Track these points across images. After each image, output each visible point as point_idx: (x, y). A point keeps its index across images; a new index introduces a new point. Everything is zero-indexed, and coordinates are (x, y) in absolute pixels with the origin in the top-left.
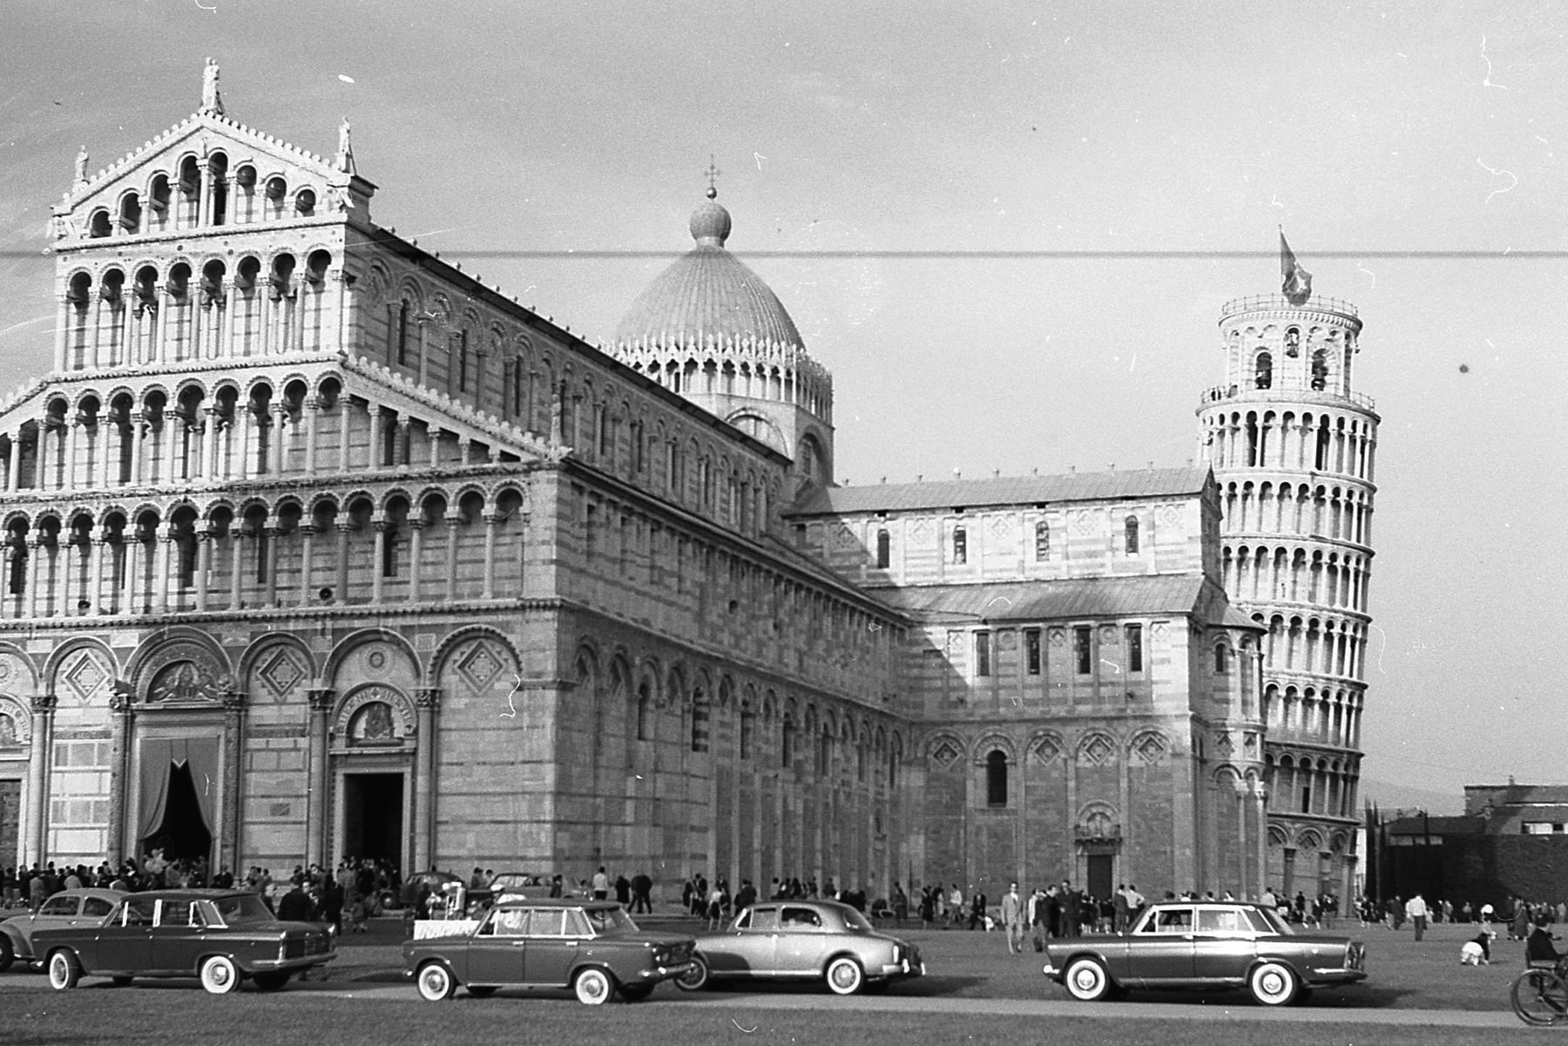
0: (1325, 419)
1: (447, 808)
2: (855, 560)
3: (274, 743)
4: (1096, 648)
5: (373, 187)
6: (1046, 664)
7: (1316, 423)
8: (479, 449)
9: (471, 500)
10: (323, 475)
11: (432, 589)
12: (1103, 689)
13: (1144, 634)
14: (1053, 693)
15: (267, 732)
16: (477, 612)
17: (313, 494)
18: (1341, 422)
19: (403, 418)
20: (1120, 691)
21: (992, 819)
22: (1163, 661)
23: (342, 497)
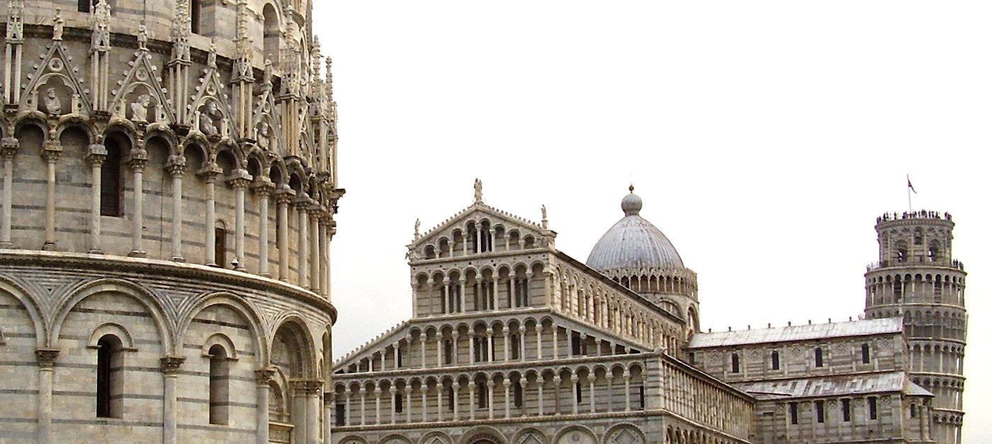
0: (938, 277)
2: (721, 369)
4: (853, 410)
5: (556, 233)
6: (827, 417)
7: (934, 279)
8: (620, 349)
9: (617, 370)
10: (545, 361)
11: (599, 407)
12: (857, 428)
13: (877, 402)
14: (831, 431)
16: (625, 417)
17: (543, 369)
18: (947, 278)
19: (583, 336)
20: (867, 429)
22: (887, 414)
23: (556, 370)
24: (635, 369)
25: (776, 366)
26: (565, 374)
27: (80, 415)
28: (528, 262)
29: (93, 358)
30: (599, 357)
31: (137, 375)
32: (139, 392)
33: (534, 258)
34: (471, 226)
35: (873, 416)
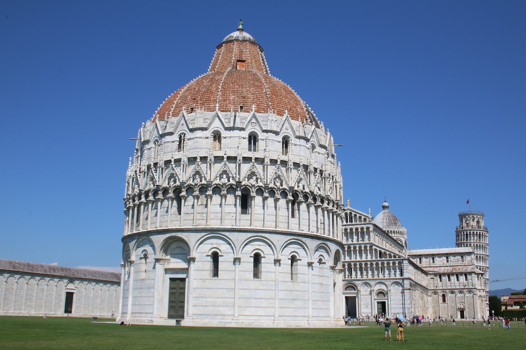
1: (392, 306)
3: (365, 297)
15: (363, 295)
21: (443, 305)
24: (400, 263)
25: (434, 262)
26: (377, 264)
27: (286, 280)
28: (365, 227)
29: (290, 262)
30: (388, 259)
31: (301, 267)
32: (302, 273)
33: (367, 225)
34: (346, 214)
35: (466, 280)
